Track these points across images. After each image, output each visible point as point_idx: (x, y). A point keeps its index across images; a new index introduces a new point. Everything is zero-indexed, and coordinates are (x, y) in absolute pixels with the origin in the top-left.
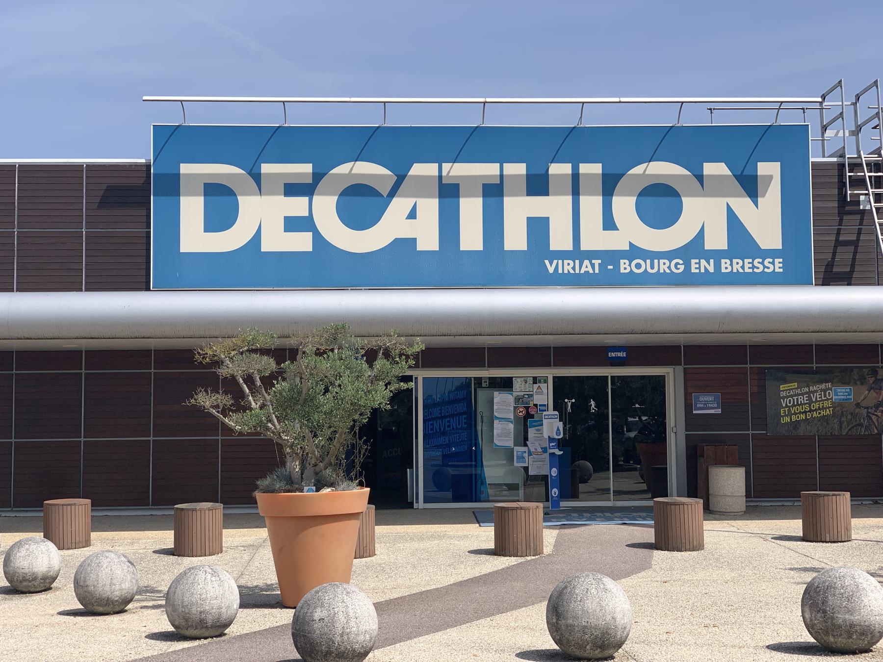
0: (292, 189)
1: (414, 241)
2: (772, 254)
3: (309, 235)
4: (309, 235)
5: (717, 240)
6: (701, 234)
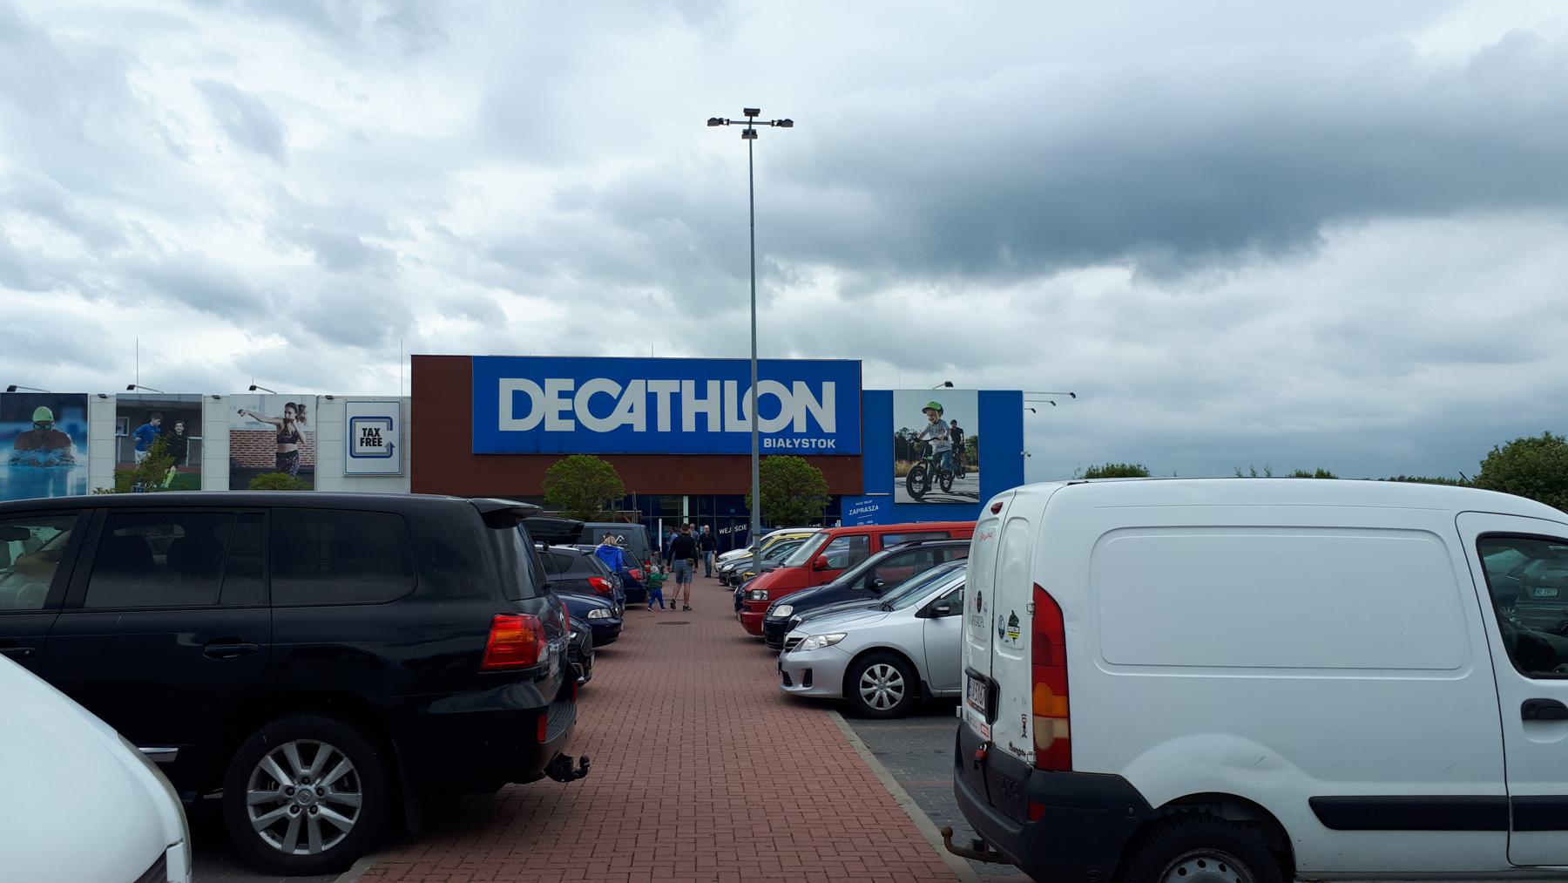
0: (563, 395)
1: (631, 426)
2: (828, 436)
3: (573, 421)
4: (573, 421)
5: (800, 427)
6: (792, 424)
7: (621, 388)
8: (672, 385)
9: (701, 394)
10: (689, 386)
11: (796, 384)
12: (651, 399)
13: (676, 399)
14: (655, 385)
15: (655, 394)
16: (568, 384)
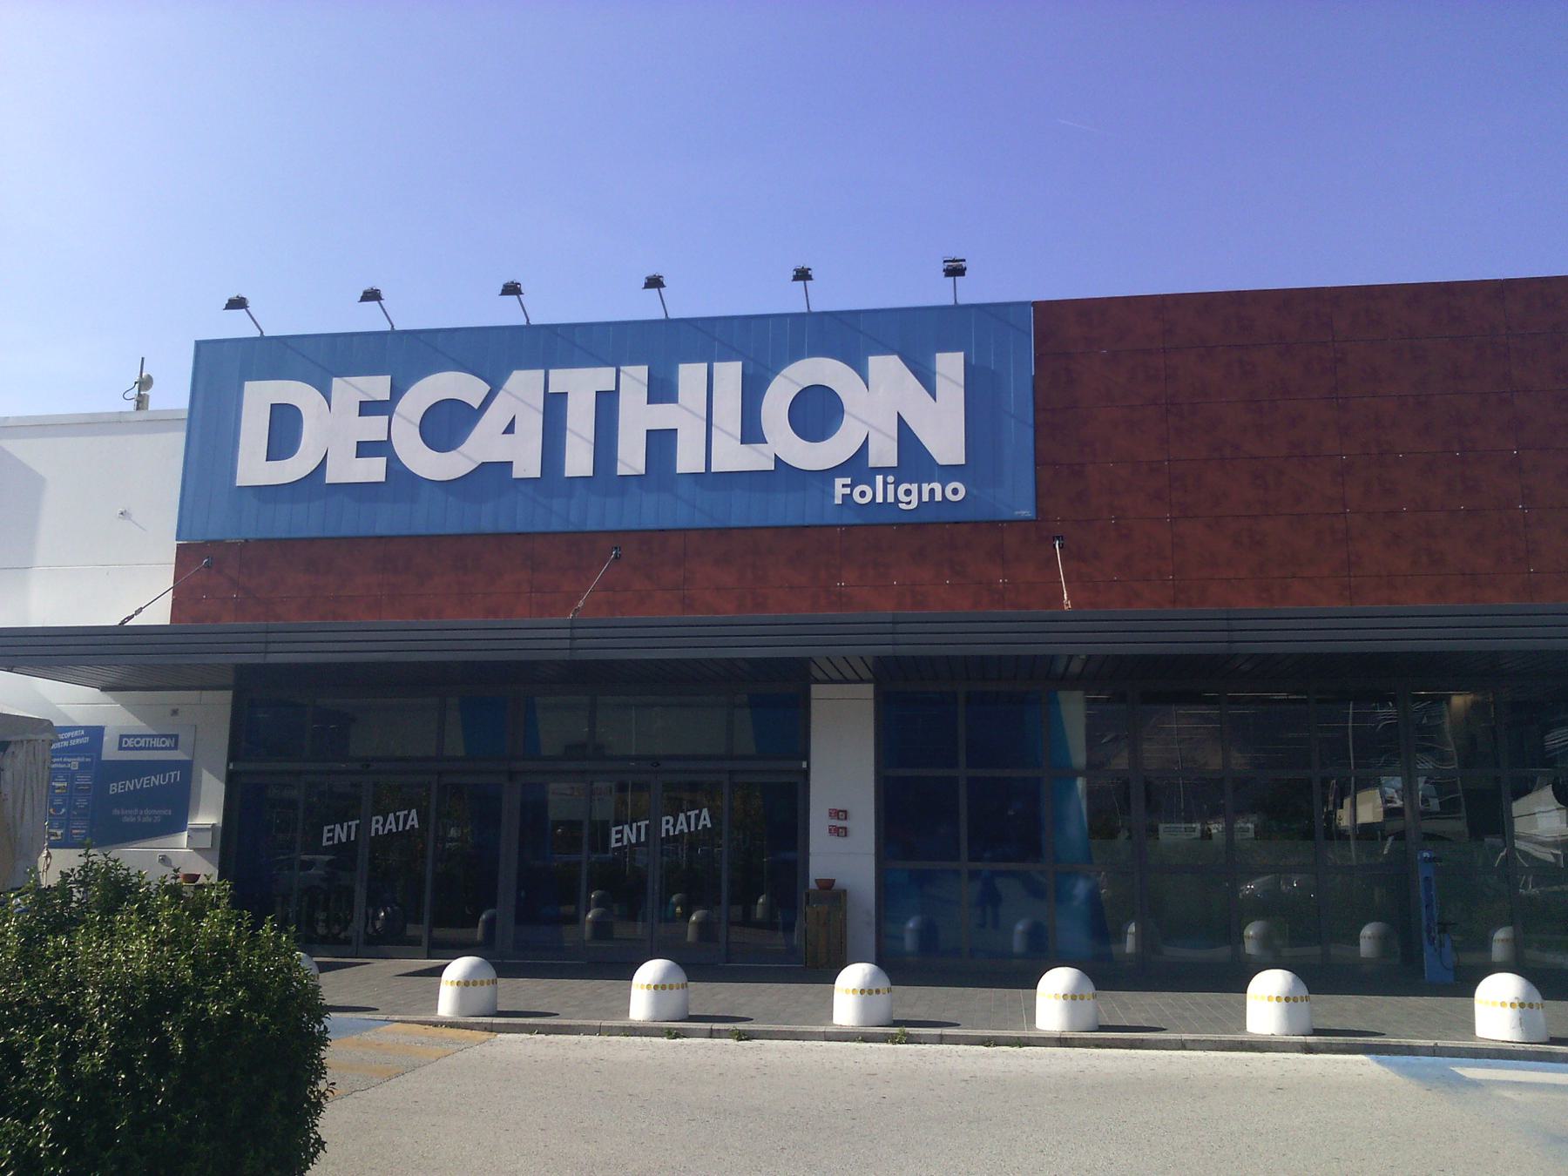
0: (367, 408)
5: (884, 453)
7: (487, 388)
8: (603, 378)
9: (662, 390)
10: (635, 378)
11: (876, 363)
12: (555, 406)
13: (607, 403)
14: (561, 379)
15: (563, 396)
16: (379, 387)
